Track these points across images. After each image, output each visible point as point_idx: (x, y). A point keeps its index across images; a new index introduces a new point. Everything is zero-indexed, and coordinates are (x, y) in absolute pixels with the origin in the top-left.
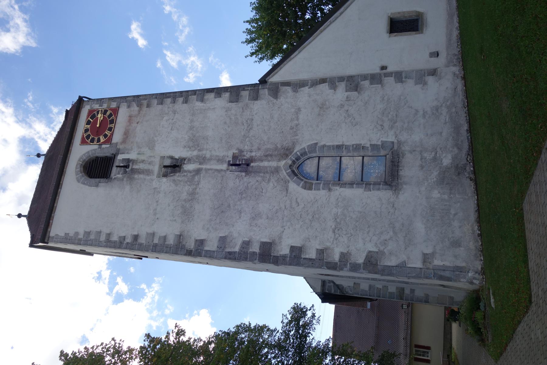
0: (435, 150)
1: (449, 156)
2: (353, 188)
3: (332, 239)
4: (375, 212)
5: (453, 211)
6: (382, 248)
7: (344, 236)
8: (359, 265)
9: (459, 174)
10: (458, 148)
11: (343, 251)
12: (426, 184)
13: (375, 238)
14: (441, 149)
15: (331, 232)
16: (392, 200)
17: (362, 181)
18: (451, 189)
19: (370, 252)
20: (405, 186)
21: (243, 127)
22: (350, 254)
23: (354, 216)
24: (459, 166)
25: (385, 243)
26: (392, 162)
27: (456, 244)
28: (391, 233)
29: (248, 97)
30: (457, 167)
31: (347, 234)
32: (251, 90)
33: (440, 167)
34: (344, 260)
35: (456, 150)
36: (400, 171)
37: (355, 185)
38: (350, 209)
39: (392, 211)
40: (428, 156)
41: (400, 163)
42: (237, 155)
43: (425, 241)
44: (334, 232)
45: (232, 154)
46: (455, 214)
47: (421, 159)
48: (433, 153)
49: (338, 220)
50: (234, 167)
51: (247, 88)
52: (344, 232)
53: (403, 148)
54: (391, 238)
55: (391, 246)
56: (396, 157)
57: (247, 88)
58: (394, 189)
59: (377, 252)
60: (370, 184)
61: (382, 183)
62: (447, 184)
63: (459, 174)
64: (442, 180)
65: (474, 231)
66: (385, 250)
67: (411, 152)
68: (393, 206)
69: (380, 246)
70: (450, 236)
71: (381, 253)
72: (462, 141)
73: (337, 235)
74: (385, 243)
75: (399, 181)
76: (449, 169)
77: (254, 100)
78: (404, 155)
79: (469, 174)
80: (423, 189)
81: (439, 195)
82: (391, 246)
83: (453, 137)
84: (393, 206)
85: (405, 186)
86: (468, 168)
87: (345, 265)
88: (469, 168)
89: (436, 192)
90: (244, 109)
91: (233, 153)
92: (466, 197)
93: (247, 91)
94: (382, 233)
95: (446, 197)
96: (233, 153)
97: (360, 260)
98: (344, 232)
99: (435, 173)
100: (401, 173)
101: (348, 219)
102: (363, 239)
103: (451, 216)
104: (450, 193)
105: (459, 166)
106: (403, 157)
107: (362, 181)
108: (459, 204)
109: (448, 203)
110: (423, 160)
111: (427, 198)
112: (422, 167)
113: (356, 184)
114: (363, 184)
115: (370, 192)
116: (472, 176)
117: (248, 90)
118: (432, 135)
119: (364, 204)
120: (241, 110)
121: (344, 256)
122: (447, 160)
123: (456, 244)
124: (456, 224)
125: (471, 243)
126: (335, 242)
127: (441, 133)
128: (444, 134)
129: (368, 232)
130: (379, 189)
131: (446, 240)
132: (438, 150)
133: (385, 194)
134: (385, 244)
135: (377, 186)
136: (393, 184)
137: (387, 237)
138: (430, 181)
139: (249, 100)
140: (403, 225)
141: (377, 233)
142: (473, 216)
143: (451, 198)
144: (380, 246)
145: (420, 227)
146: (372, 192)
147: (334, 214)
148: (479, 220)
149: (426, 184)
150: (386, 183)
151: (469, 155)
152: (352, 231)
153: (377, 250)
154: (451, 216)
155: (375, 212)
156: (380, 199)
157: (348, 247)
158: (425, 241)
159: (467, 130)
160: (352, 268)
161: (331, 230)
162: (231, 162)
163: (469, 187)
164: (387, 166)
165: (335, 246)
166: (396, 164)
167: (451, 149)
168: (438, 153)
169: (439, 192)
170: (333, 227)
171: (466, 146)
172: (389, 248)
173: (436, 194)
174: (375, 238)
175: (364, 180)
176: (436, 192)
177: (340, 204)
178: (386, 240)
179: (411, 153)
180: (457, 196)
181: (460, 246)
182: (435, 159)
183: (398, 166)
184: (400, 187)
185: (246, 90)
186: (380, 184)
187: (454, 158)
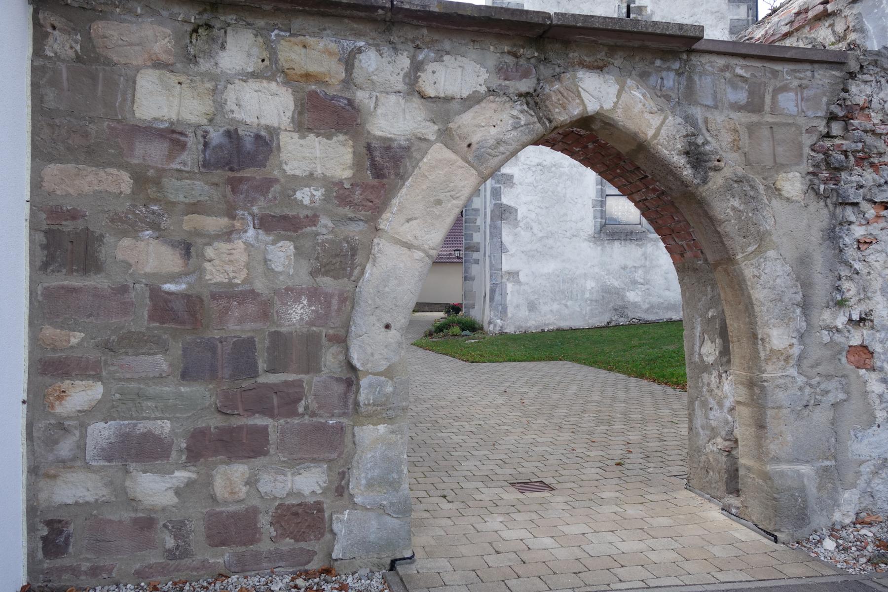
0: (647, 282)
1: (638, 299)
2: (597, 185)
3: (528, 163)
4: (565, 215)
5: (569, 303)
6: (521, 224)
7: (534, 177)
8: (499, 199)
9: (616, 310)
10: (648, 309)
11: (515, 178)
12: (603, 273)
13: (533, 216)
14: (648, 289)
15: (537, 161)
16: (582, 233)
17: (607, 195)
18: (596, 301)
19: (516, 211)
20: (599, 248)
21: (686, 16)
22: (512, 187)
23: (559, 189)
24: (626, 310)
25: (529, 228)
26: (632, 233)
27: (532, 307)
28: (540, 235)
29: (736, 17)
30: (624, 307)
31: (536, 181)
32: (748, 21)
33: (624, 289)
34: (504, 179)
35: (646, 306)
36: (620, 242)
37: (600, 187)
38: (569, 183)
39: (568, 234)
40: (639, 275)
41: (629, 241)
42: (644, 13)
43: (533, 273)
44: (538, 165)
45: (645, 5)
46: (566, 306)
47: (635, 267)
48: (642, 281)
49: (553, 169)
50: (625, 10)
51: (750, 15)
52: (538, 178)
53: (649, 245)
54: (534, 234)
55: (525, 235)
56: (638, 237)
57: (750, 15)
58: (596, 236)
59: (516, 219)
60: (602, 206)
61: (604, 221)
62: (603, 297)
63: (616, 310)
64: (608, 291)
65: (547, 325)
66: (519, 229)
67: (644, 254)
68: (574, 236)
69: (524, 222)
70: (541, 301)
71: (516, 223)
72: (657, 313)
73: (534, 169)
74: (529, 228)
75: (607, 242)
76: (622, 299)
77: (731, 29)
78: (640, 246)
79: (615, 321)
80: (597, 270)
81: (589, 287)
82: (525, 235)
83: (662, 303)
84: (574, 236)
85: (599, 248)
86: (623, 319)
87: (498, 182)
88: (622, 321)
89: (593, 284)
90: (717, 14)
91: (646, 7)
92: (587, 318)
93: (746, 14)
94: (540, 223)
95: (587, 295)
96: (646, 7)
97: (505, 200)
98: (538, 178)
99: (616, 284)
100: (617, 243)
101: (556, 181)
102: (531, 202)
103: (564, 302)
104: (592, 301)
105: (626, 310)
106: (637, 245)
107: (607, 195)
108: (579, 310)
109: (579, 297)
110: (633, 269)
111: (585, 274)
112: (624, 268)
113: (602, 189)
114: (602, 197)
115: (591, 206)
116: (613, 324)
117: (748, 16)
118: (666, 279)
119: (576, 200)
120: (716, 9)
121: (508, 180)
122: (632, 296)
123: (532, 307)
124: (555, 307)
125: (534, 322)
126: (525, 167)
127: (669, 290)
128: (667, 293)
129: (539, 207)
130: (595, 217)
131: (536, 297)
132: (647, 287)
133: (589, 223)
134: (527, 228)
135: (599, 215)
136: (602, 234)
137: (535, 230)
138: (606, 277)
139: (731, 20)
140: (552, 248)
141: (540, 218)
142: (565, 324)
143: (586, 301)
144: (524, 222)
145: (550, 267)
146: (592, 210)
147: (561, 163)
148: (559, 331)
149: (603, 273)
150: (603, 226)
151: (640, 320)
152: (540, 187)
153: (518, 219)
154: (564, 302)
155: (565, 215)
156: (582, 219)
157: (520, 184)
158: (533, 273)
159: (671, 319)
160: (496, 190)
161: (541, 161)
162: (632, 5)
163: (600, 320)
164: (627, 226)
165: (521, 168)
166: (629, 237)
167: (647, 301)
168: (642, 286)
169: (592, 288)
170: (545, 163)
171: (651, 317)
172: (523, 233)
173: (590, 284)
174: (533, 216)
175: (608, 197)
176: (593, 284)
177: (575, 169)
178: (531, 229)
179: (643, 255)
180: (588, 308)
181: (530, 310)
182: (635, 282)
183: (626, 240)
184: (598, 243)
185: (748, 13)
186: (602, 218)
187: (636, 305)
